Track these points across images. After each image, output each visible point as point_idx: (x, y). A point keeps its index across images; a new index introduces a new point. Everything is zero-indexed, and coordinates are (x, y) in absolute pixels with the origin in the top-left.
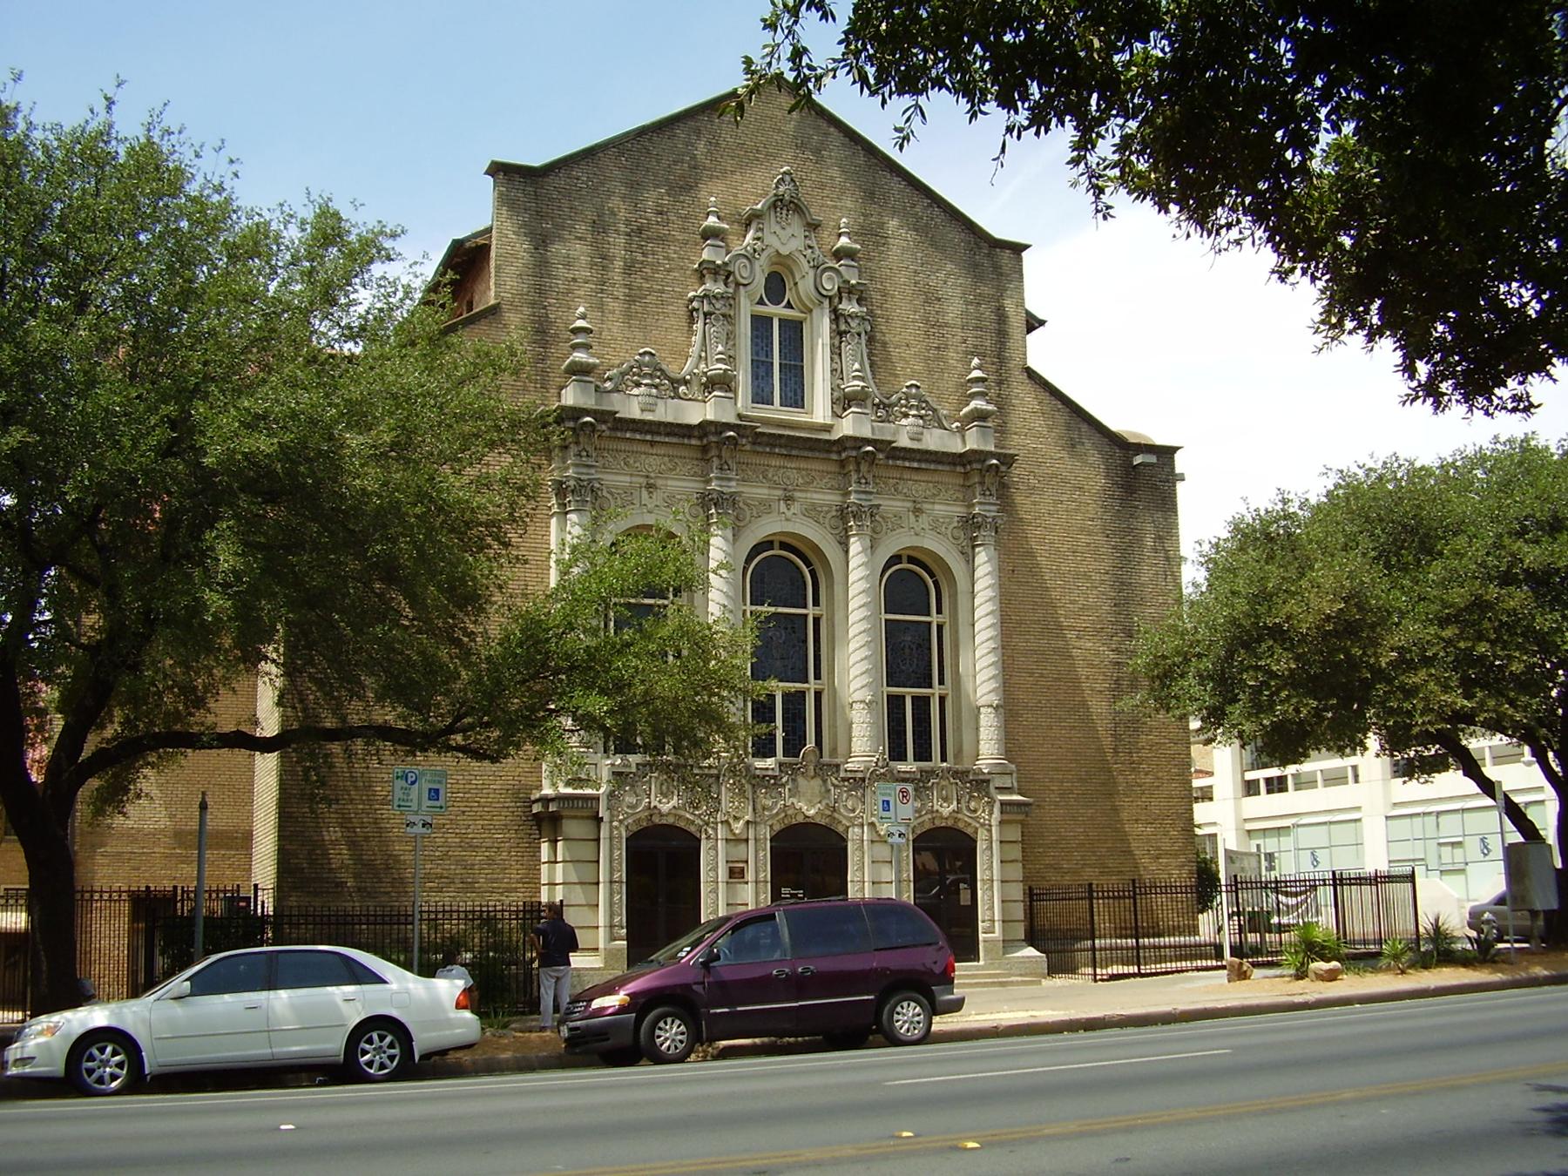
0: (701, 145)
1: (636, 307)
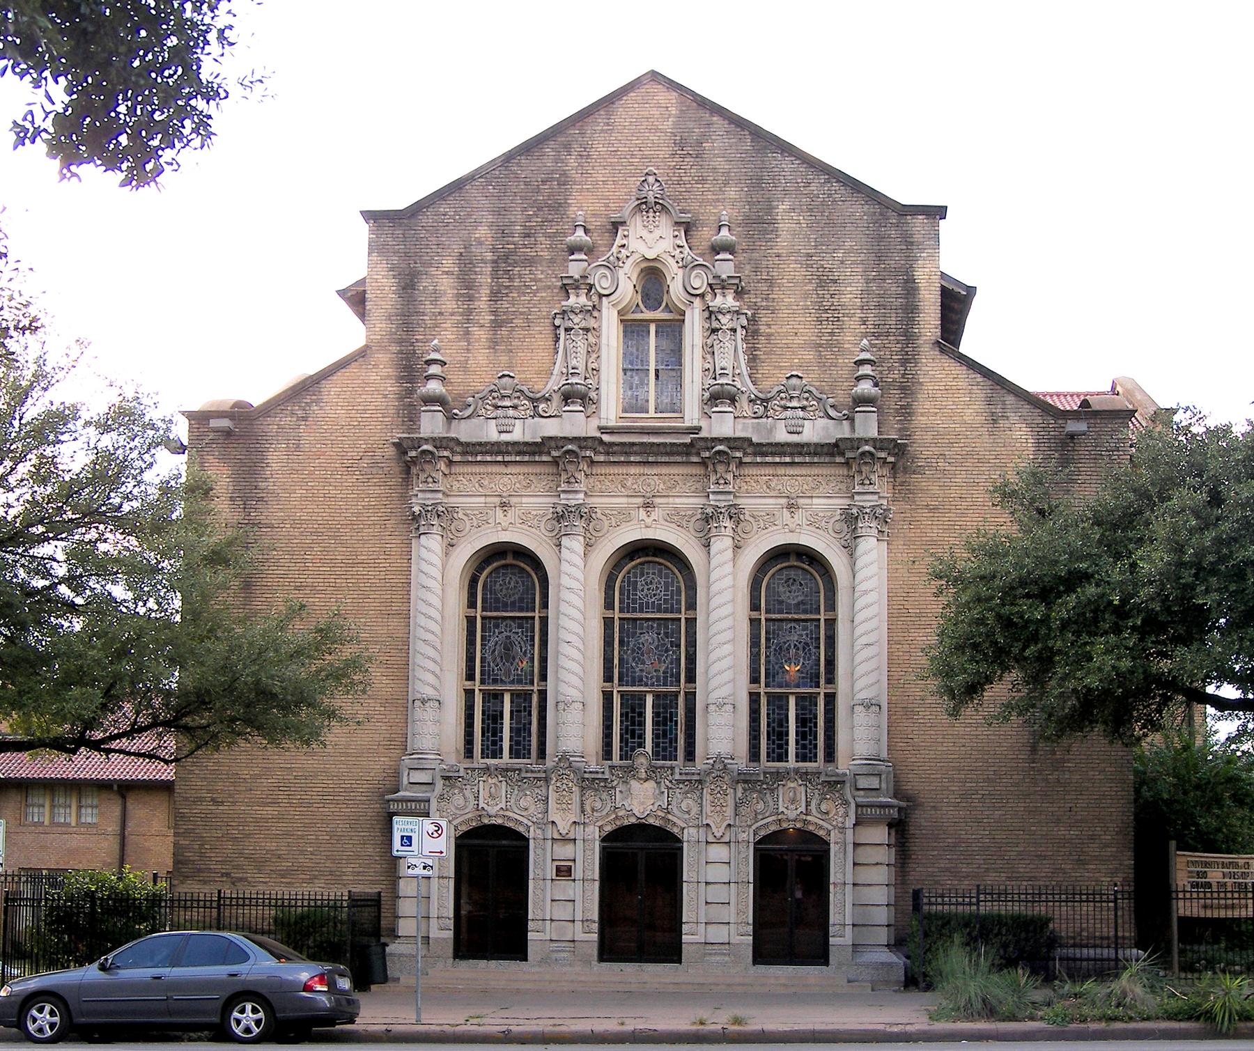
0: (573, 161)
1: (504, 331)
